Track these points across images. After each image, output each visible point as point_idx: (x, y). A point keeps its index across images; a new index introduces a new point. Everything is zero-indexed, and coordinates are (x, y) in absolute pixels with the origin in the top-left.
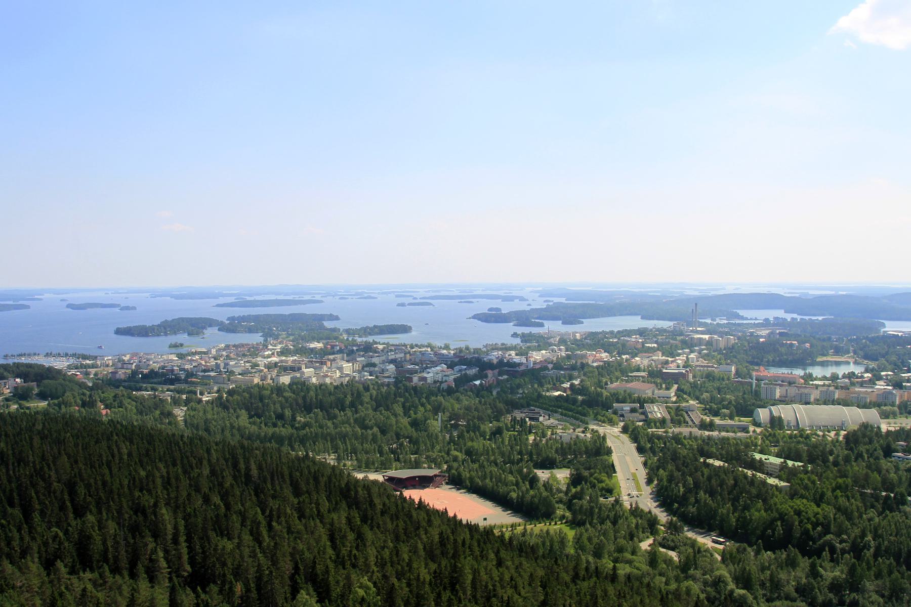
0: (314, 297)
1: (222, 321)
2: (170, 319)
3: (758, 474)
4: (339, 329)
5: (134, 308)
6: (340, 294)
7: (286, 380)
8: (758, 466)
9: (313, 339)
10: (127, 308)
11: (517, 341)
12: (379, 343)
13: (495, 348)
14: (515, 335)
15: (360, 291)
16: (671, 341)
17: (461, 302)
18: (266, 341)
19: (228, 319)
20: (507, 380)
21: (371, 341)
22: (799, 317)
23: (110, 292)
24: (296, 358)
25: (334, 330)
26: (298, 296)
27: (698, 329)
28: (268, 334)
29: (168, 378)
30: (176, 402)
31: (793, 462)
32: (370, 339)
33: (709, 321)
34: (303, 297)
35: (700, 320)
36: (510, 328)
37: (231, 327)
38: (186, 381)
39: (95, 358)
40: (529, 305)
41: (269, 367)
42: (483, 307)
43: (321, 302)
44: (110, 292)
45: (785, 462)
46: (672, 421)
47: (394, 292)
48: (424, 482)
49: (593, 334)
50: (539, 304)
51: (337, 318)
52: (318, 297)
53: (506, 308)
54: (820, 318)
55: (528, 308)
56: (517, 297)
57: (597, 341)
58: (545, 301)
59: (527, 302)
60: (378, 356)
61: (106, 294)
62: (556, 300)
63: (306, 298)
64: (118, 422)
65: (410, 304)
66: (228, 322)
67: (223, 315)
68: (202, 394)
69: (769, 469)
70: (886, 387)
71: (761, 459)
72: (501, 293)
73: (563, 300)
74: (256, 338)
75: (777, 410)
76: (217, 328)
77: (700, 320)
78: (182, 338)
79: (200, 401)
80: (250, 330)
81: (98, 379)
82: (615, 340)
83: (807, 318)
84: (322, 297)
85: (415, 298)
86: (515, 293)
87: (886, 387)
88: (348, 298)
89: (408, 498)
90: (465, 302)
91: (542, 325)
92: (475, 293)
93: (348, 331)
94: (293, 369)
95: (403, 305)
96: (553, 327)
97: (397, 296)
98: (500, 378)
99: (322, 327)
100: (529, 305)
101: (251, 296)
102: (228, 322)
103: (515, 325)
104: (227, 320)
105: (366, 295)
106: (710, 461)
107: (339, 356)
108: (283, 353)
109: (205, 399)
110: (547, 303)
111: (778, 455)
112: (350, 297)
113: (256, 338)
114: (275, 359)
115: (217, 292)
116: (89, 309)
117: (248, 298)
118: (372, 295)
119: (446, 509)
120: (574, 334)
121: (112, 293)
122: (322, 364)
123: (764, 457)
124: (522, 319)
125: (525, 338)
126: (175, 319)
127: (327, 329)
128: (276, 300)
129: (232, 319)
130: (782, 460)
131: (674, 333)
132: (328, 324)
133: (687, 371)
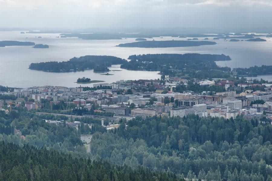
1: (124, 60)
2: (78, 56)
5: (46, 47)
6: (230, 36)
7: (181, 113)
9: (206, 77)
10: (40, 46)
12: (267, 82)
15: (250, 34)
18: (163, 77)
19: (130, 57)
21: (260, 80)
23: (25, 32)
24: (190, 94)
25: (227, 69)
28: (164, 73)
29: (76, 110)
30: (84, 131)
32: (259, 78)
38: (92, 112)
39: (12, 90)
41: (167, 101)
43: (214, 43)
44: (25, 32)
51: (228, 58)
52: (211, 39)
60: (265, 94)
61: (22, 33)
63: (200, 39)
64: (32, 147)
66: (130, 60)
67: (125, 54)
68: (106, 124)
74: (154, 76)
76: (119, 66)
78: (89, 74)
79: (105, 130)
80: (150, 69)
81: (15, 108)
84: (214, 39)
88: (238, 41)
94: (187, 104)
99: (215, 66)
101: (150, 37)
102: (130, 60)
104: (129, 59)
105: (255, 38)
107: (229, 93)
108: (177, 90)
109: (110, 128)
112: (240, 39)
113: (154, 76)
114: (171, 95)
115: (120, 33)
116: (6, 46)
117: (148, 39)
118: (262, 38)
121: (27, 33)
122: (214, 100)
126: (83, 57)
127: (218, 68)
128: (173, 41)
129: (132, 57)
132: (220, 64)
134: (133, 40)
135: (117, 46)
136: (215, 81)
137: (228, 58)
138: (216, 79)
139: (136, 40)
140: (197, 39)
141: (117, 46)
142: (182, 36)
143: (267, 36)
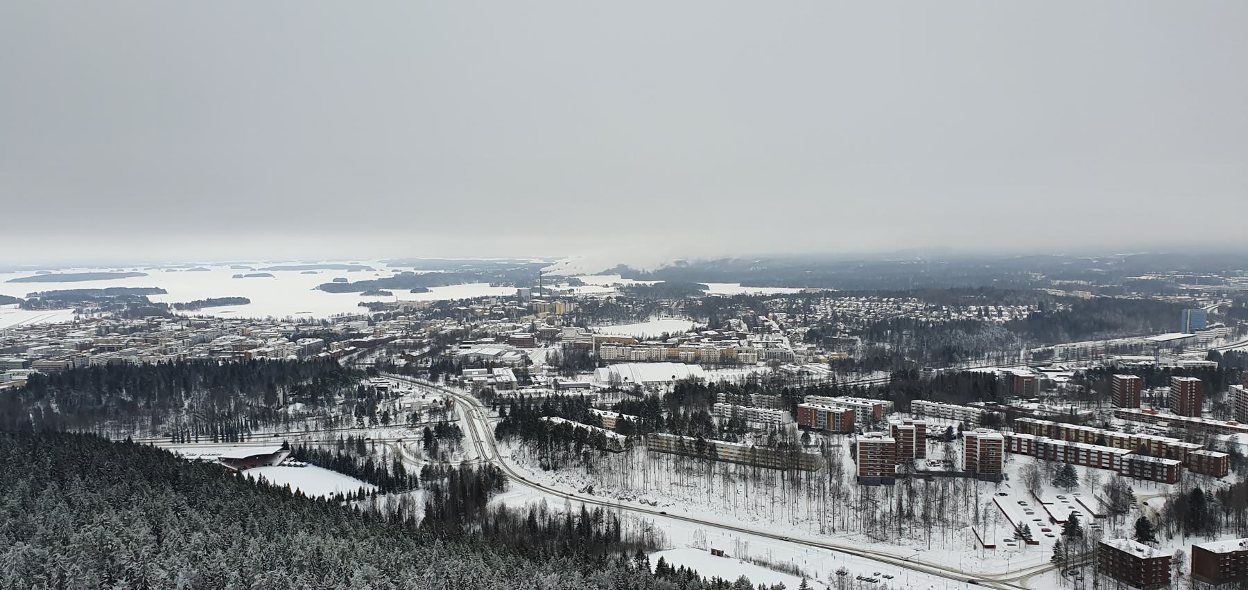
0: (136, 270)
3: (597, 428)
4: (167, 304)
6: (166, 266)
8: (598, 421)
11: (365, 311)
13: (339, 319)
16: (518, 308)
17: (305, 273)
19: (29, 295)
20: (355, 351)
22: (634, 283)
26: (115, 269)
31: (627, 416)
33: (553, 287)
34: (123, 270)
36: (357, 297)
37: (32, 304)
40: (377, 275)
42: (328, 277)
45: (621, 416)
46: (519, 382)
47: (229, 264)
48: (265, 460)
49: (442, 303)
50: (388, 274)
51: (164, 292)
52: (141, 270)
53: (352, 278)
54: (653, 283)
55: (376, 278)
56: (363, 267)
57: (446, 309)
59: (375, 273)
62: (405, 270)
63: (126, 270)
65: (246, 276)
66: (28, 299)
67: (21, 292)
70: (709, 344)
73: (411, 270)
75: (614, 368)
82: (464, 308)
83: (641, 283)
85: (254, 270)
86: (362, 263)
87: (709, 344)
88: (176, 271)
89: (302, 493)
90: (307, 273)
91: (390, 294)
92: (319, 263)
93: (179, 306)
95: (240, 276)
96: (403, 296)
97: (232, 268)
98: (347, 349)
100: (377, 275)
105: (197, 267)
106: (554, 419)
110: (395, 273)
111: (614, 409)
112: (178, 269)
117: (54, 272)
119: (288, 484)
123: (602, 412)
124: (368, 287)
125: (374, 306)
127: (151, 304)
130: (618, 415)
131: (519, 299)
133: (532, 336)
134: (33, 274)
135: (7, 282)
136: (148, 320)
137: (164, 292)
138: (149, 317)
139: (36, 273)
140: (123, 270)
141: (7, 282)
142: (101, 268)
143: (211, 265)
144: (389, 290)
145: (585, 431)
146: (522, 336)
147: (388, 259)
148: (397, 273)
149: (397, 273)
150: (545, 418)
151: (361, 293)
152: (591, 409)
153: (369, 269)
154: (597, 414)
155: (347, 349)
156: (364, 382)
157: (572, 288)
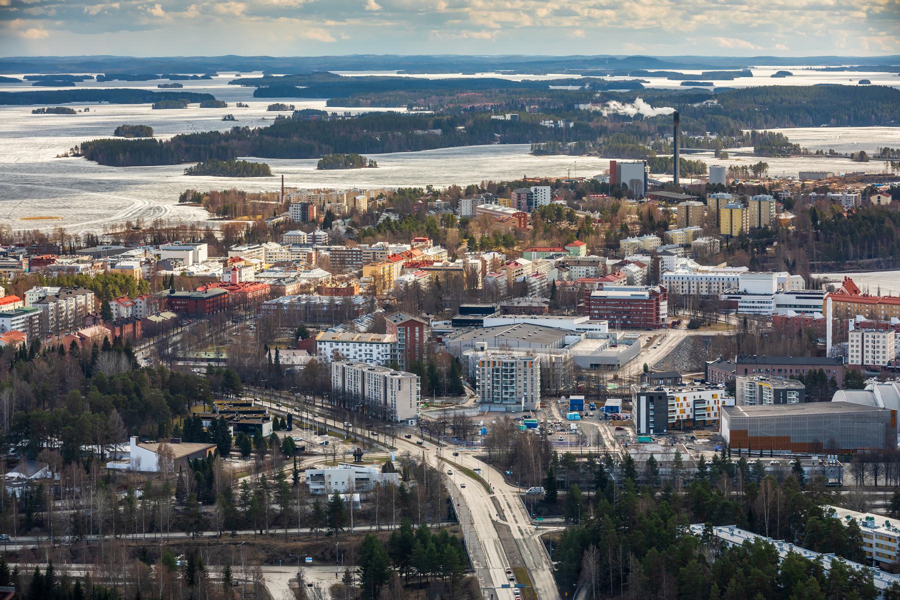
3: (848, 563)
14: (190, 198)
20: (175, 323)
27: (682, 181)
33: (708, 159)
35: (687, 158)
55: (226, 128)
58: (271, 108)
69: (875, 549)
71: (853, 523)
72: (152, 86)
77: (687, 158)
86: (188, 87)
91: (264, 172)
103: (190, 172)
106: (723, 533)
110: (276, 113)
120: (353, 194)
133: (653, 294)
144: (261, 161)
145: (815, 568)
146: (627, 294)
147: (259, 75)
148: (282, 113)
149: (282, 113)
150: (698, 529)
151: (188, 166)
152: (826, 508)
153: (208, 100)
154: (845, 523)
155: (153, 318)
156: (199, 409)
157: (764, 160)
